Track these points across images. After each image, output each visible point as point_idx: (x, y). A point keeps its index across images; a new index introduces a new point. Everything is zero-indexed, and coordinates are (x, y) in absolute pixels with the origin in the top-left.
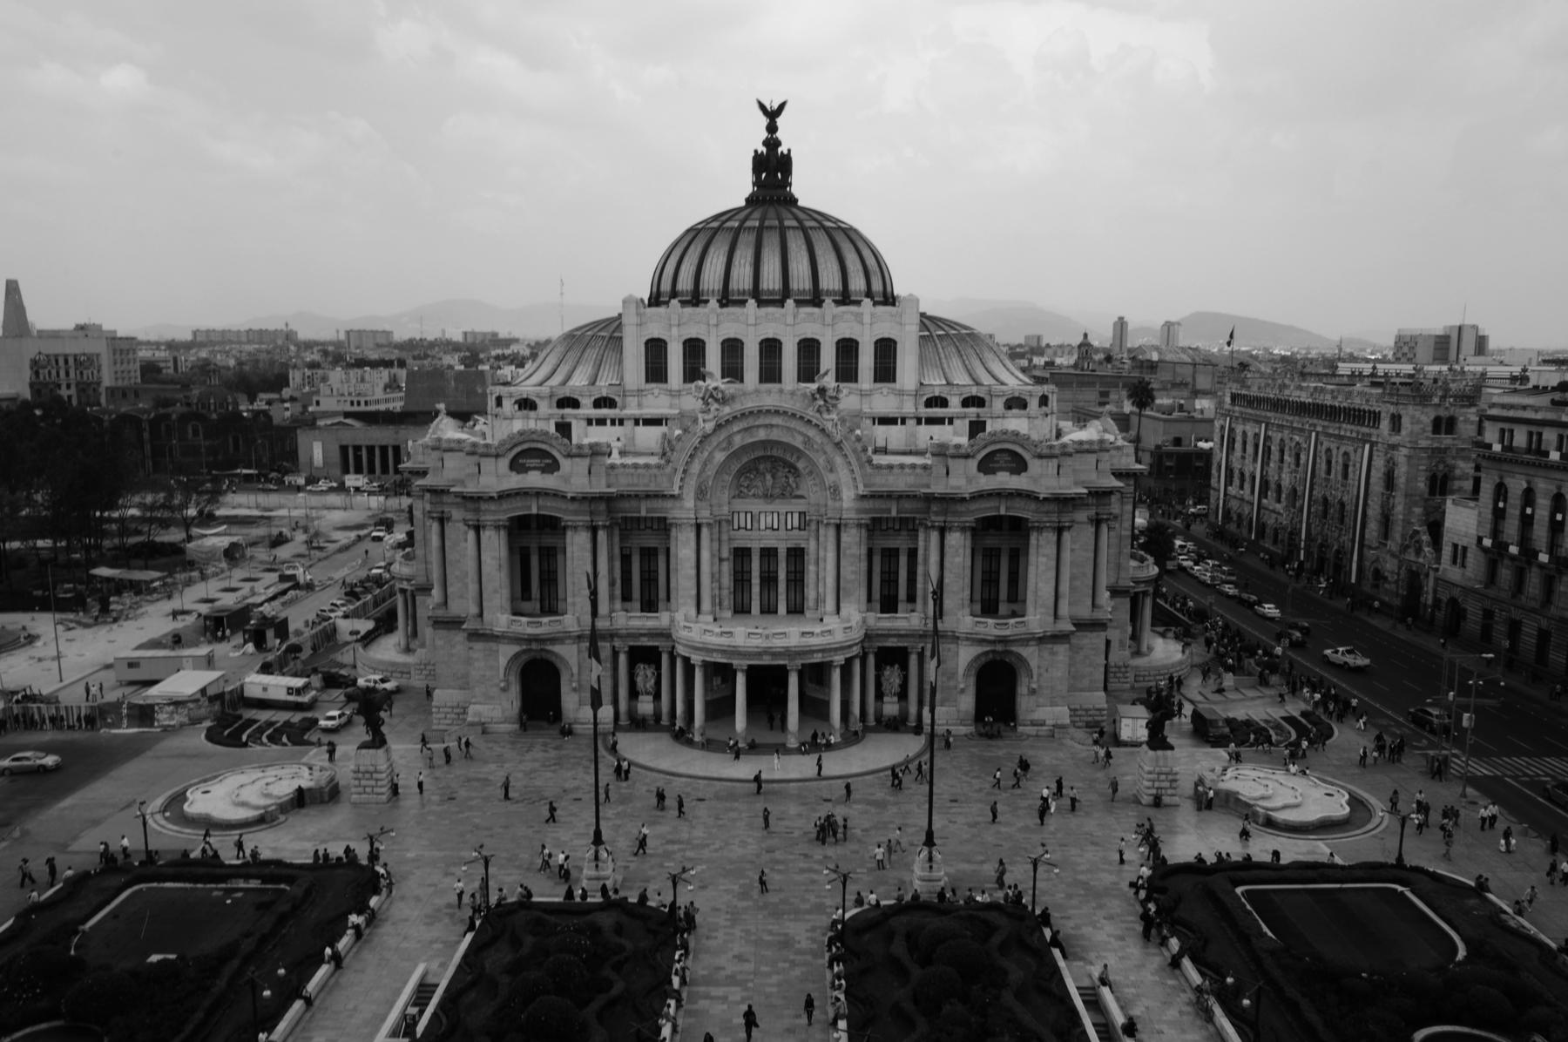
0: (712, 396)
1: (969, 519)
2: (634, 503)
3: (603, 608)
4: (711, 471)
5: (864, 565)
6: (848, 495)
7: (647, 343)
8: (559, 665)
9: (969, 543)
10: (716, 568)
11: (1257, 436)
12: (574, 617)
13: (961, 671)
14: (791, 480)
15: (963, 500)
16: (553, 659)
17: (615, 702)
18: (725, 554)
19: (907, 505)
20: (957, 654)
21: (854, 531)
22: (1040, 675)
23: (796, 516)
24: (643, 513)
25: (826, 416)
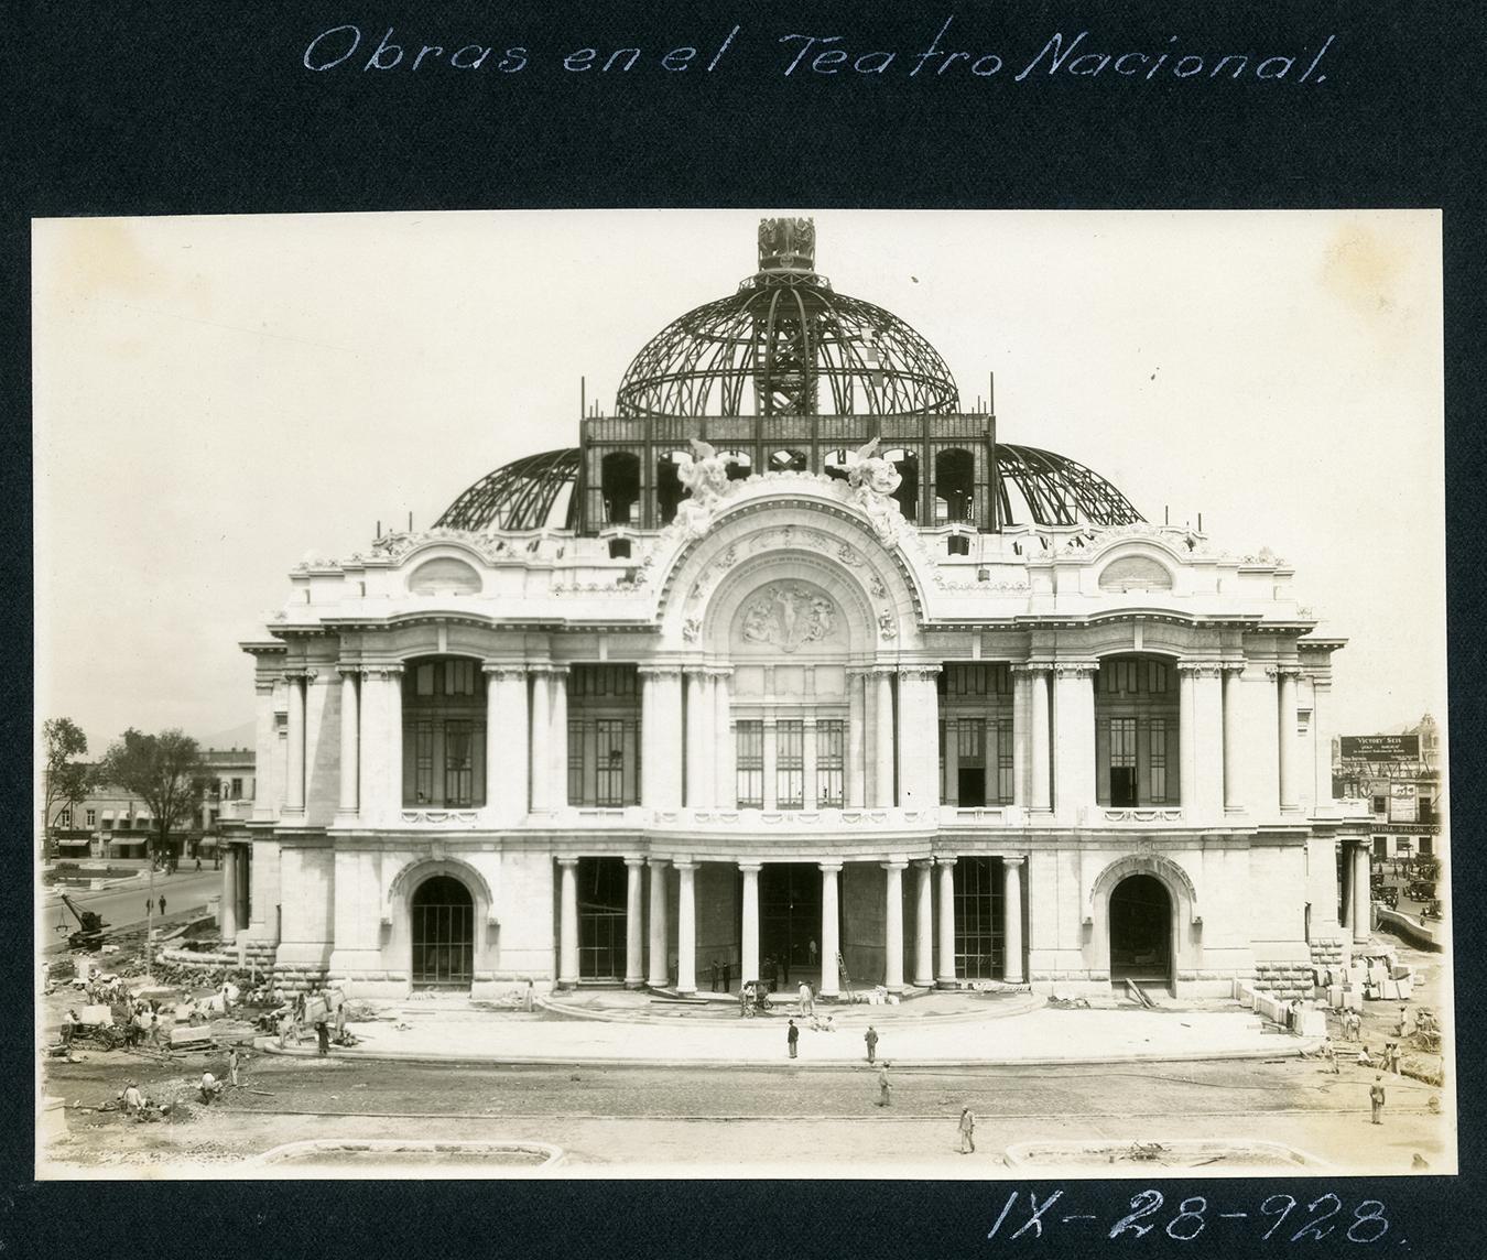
1: (1091, 661)
2: (588, 642)
8: (472, 887)
12: (502, 809)
15: (1080, 625)
16: (462, 877)
21: (918, 683)
24: (604, 658)
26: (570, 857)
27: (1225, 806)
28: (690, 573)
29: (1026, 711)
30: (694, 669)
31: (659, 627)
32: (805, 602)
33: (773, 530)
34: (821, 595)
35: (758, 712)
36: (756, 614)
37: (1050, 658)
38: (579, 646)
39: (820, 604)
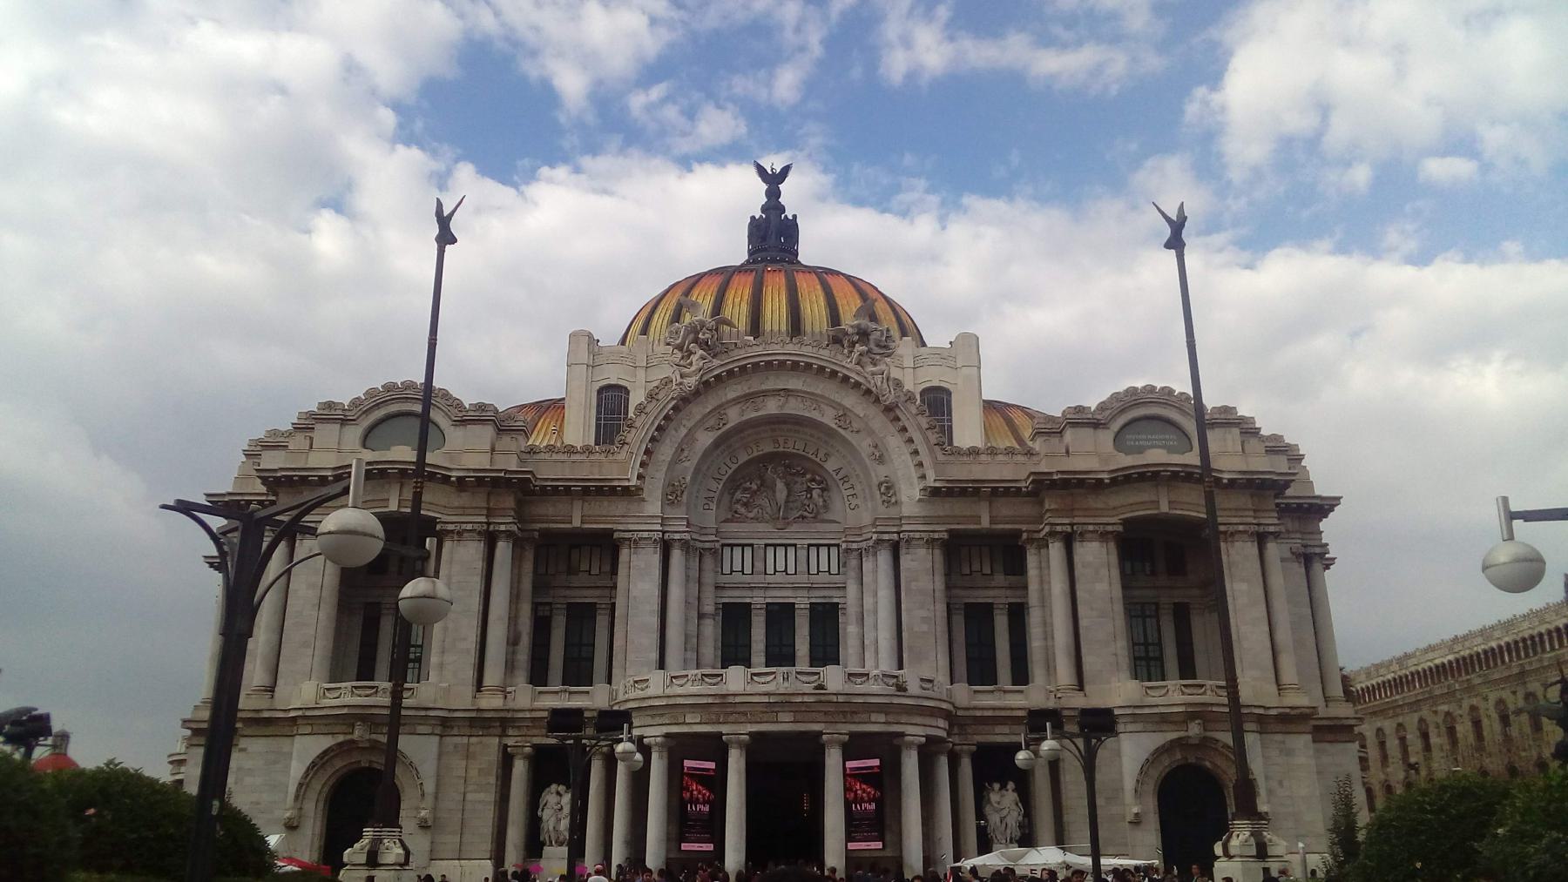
0: (696, 341)
1: (1113, 521)
3: (493, 676)
4: (690, 465)
5: (941, 608)
6: (910, 494)
7: (600, 391)
9: (1114, 559)
10: (693, 628)
11: (1380, 731)
13: (1129, 783)
14: (815, 493)
17: (498, 857)
18: (709, 608)
19: (1006, 509)
20: (1118, 754)
21: (922, 552)
22: (1270, 792)
23: (823, 551)
24: (577, 523)
25: (871, 368)
26: (522, 742)
27: (1278, 685)
28: (677, 434)
29: (1042, 582)
30: (677, 536)
31: (639, 489)
32: (799, 479)
33: (765, 394)
34: (814, 473)
35: (749, 593)
36: (746, 489)
37: (1066, 521)
38: (551, 511)
39: (813, 480)
